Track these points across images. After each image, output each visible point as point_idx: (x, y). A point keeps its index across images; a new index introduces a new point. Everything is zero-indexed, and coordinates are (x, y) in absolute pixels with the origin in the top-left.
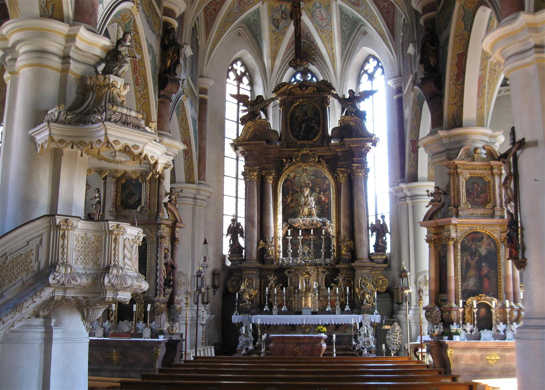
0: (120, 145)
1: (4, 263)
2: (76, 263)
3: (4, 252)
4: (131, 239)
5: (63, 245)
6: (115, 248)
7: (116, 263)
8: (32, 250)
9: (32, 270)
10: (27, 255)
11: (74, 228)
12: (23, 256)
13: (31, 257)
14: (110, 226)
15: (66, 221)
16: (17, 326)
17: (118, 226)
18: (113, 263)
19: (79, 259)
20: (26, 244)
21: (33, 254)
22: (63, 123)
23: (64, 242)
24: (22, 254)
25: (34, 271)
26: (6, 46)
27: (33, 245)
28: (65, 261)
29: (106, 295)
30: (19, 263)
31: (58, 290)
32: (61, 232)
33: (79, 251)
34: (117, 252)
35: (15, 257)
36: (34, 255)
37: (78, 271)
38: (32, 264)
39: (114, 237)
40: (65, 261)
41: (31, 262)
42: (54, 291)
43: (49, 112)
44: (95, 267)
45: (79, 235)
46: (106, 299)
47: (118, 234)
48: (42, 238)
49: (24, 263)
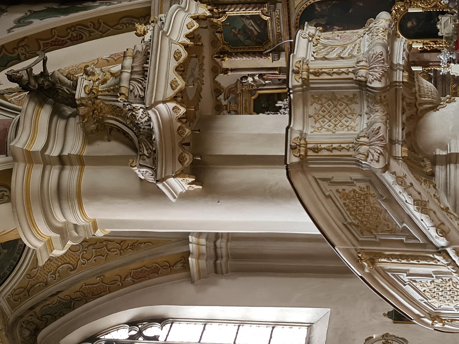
0: (177, 79)
1: (357, 226)
2: (353, 128)
3: (342, 227)
4: (313, 49)
5: (328, 150)
6: (328, 74)
7: (350, 70)
8: (337, 191)
9: (366, 190)
10: (345, 196)
11: (303, 136)
12: (347, 201)
13: (347, 191)
14: (296, 83)
15: (293, 148)
16: (446, 203)
17: (297, 72)
18: (351, 76)
19: (347, 124)
20: (330, 200)
21: (344, 190)
22: (155, 162)
23: (325, 149)
24: (344, 204)
25: (367, 187)
26: (59, 240)
27: (330, 189)
28: (351, 145)
29: (400, 82)
30: (357, 207)
31: (394, 152)
32: (310, 153)
33: (336, 125)
34: (335, 70)
35: (348, 212)
36: (344, 187)
37: (365, 126)
38: (358, 190)
39: (312, 77)
40: (351, 145)
41: (354, 191)
42: (396, 158)
43: (142, 178)
44: (358, 100)
45: (313, 127)
46: (405, 80)
47: (308, 70)
48: (319, 179)
49: (357, 201)
